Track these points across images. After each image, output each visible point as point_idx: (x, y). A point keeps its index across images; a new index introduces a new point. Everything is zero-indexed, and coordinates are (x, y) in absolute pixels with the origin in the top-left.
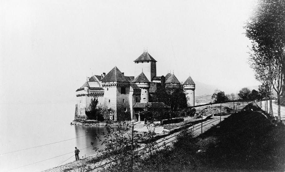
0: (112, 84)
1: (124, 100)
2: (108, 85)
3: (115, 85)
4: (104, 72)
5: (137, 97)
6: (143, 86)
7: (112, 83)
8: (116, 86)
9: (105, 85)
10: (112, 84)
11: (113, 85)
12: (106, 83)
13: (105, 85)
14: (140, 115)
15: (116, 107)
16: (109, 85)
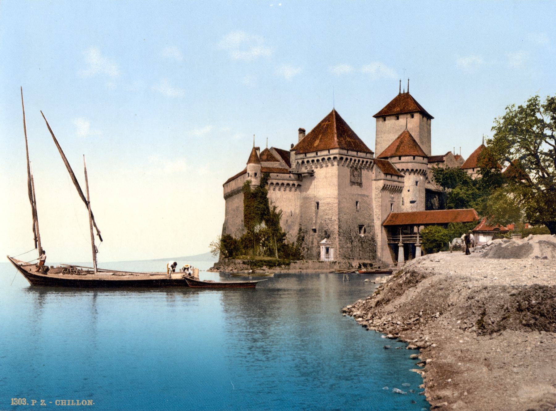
0: (326, 158)
1: (357, 202)
2: (313, 161)
3: (335, 158)
4: (302, 127)
5: (393, 198)
6: (410, 166)
7: (326, 152)
8: (335, 163)
9: (305, 160)
10: (326, 158)
11: (329, 159)
12: (308, 155)
13: (305, 160)
14: (403, 246)
15: (337, 222)
16: (315, 159)
